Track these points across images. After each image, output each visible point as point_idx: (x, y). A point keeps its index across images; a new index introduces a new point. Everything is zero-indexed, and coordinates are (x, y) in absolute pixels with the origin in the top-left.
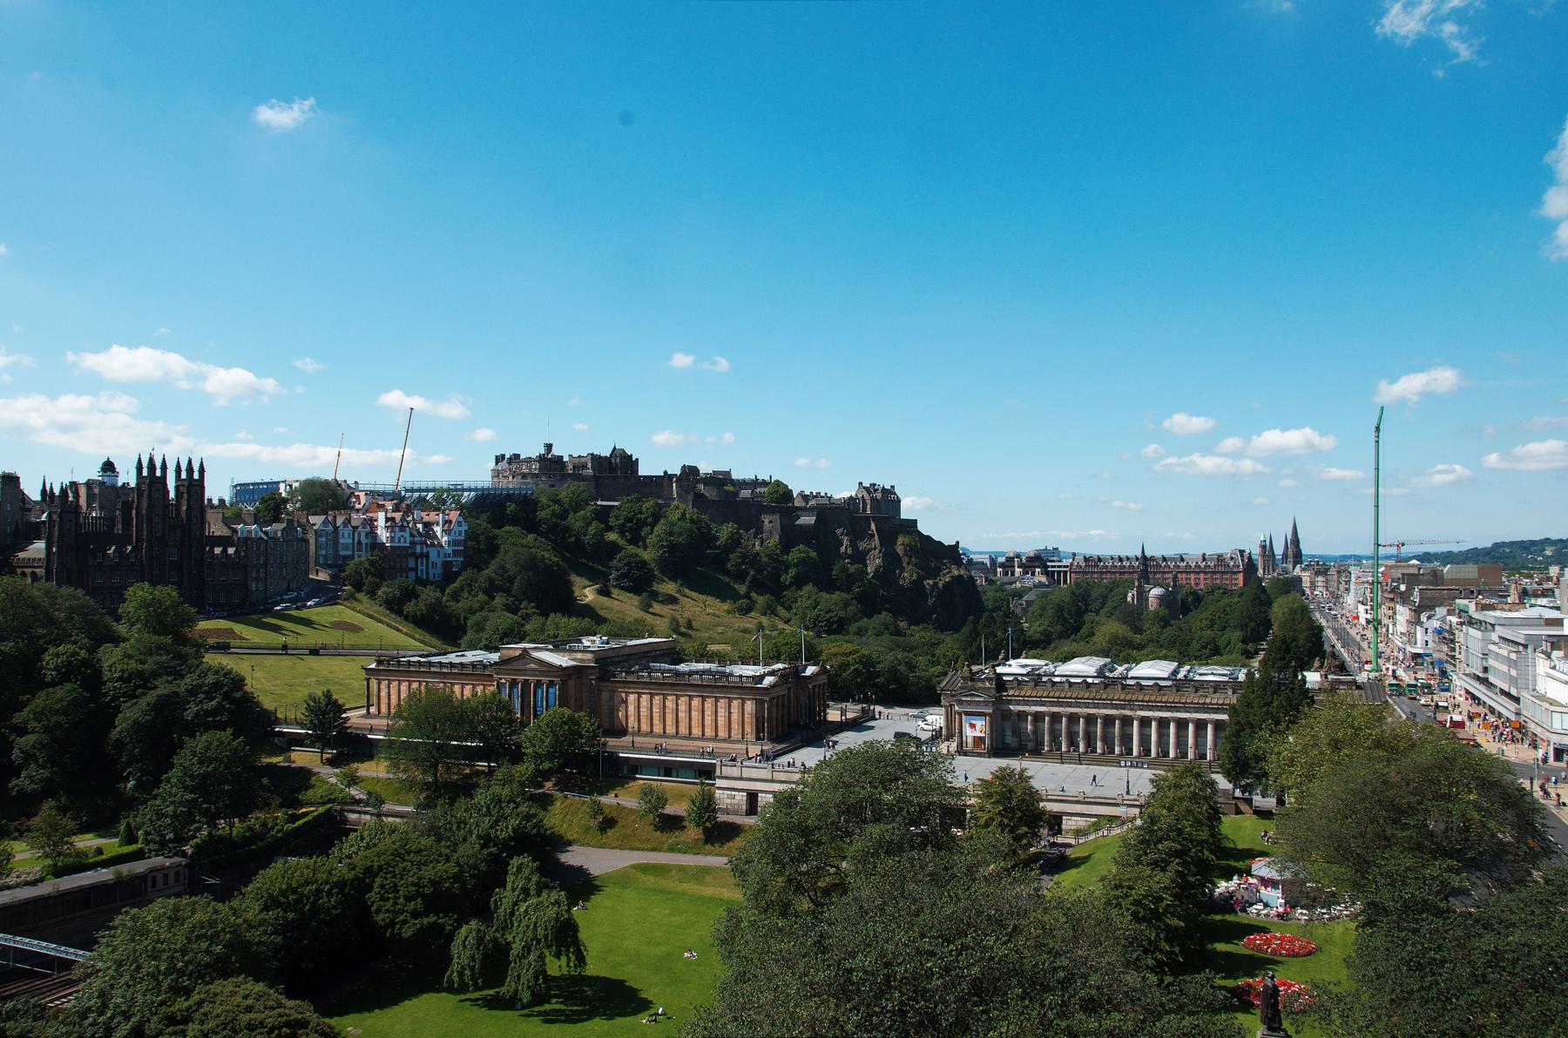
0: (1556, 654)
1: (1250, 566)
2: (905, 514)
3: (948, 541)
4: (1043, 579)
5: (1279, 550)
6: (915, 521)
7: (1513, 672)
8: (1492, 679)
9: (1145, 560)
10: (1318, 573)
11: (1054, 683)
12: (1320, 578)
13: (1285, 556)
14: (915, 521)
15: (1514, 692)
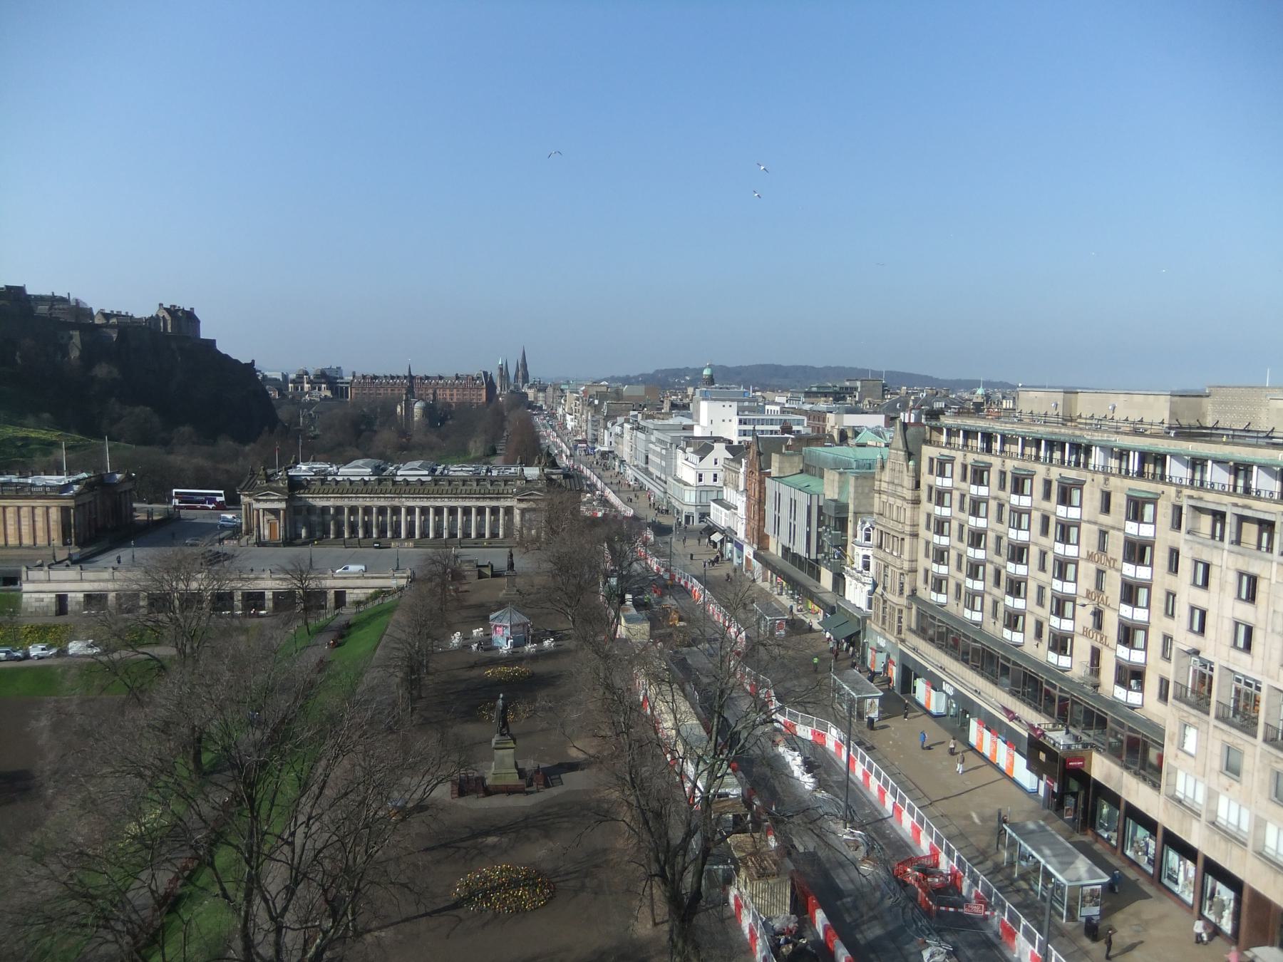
0: (689, 450)
1: (491, 386)
2: (205, 334)
3: (245, 360)
4: (329, 394)
5: (512, 373)
6: (214, 341)
7: (664, 463)
8: (651, 469)
9: (411, 378)
10: (539, 390)
11: (337, 482)
12: (541, 395)
13: (516, 376)
14: (214, 341)
15: (663, 477)
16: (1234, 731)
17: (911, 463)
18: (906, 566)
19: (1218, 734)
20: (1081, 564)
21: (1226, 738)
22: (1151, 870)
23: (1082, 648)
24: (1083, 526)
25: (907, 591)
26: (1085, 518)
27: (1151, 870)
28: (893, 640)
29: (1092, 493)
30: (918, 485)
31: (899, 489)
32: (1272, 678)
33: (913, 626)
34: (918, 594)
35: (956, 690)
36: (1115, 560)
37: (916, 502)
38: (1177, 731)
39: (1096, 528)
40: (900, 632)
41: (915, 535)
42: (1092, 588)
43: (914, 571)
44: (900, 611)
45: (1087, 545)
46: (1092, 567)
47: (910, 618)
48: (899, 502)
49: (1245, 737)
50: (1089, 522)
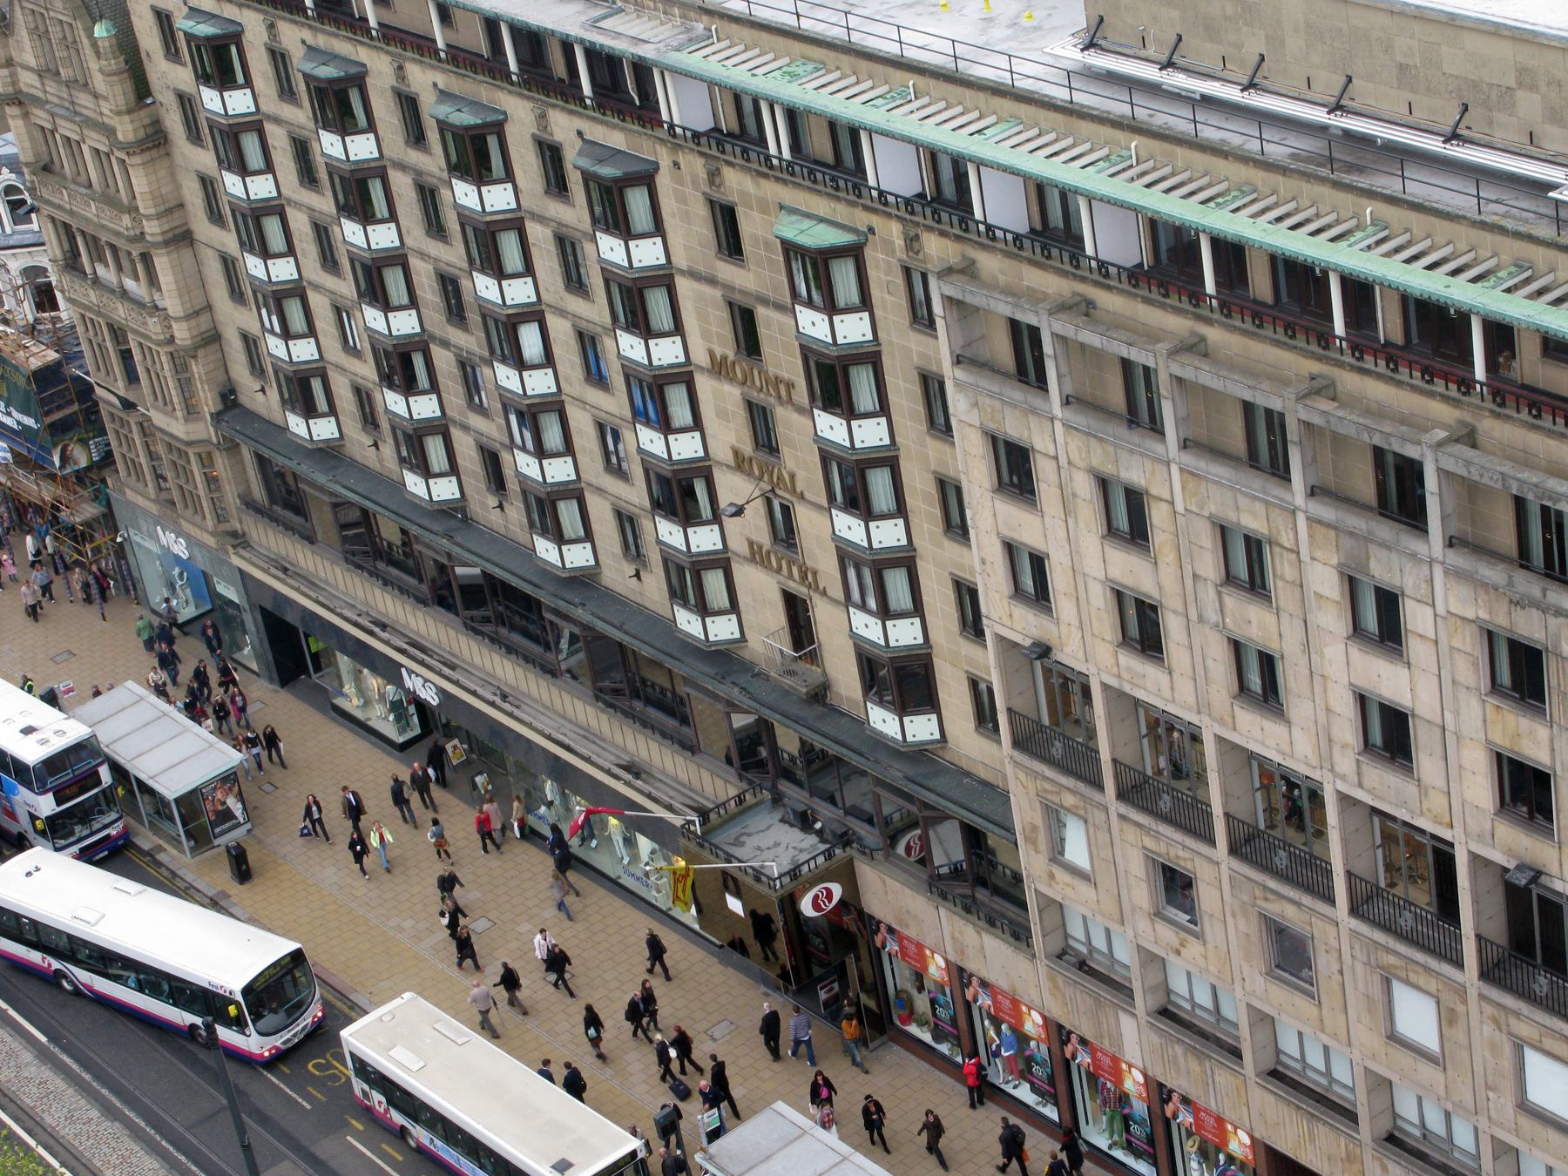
16: (1164, 829)
17: (100, 30)
18: (182, 333)
19: (1131, 834)
20: (703, 384)
21: (1149, 842)
22: (1051, 1112)
23: (761, 589)
24: (683, 285)
25: (208, 401)
26: (680, 261)
27: (1051, 1112)
28: (211, 541)
29: (682, 200)
30: (142, 90)
31: (84, 99)
32: (1221, 722)
33: (258, 492)
34: (244, 400)
35: (442, 692)
36: (790, 386)
37: (155, 140)
38: (1038, 820)
39: (717, 293)
40: (220, 518)
41: (183, 238)
42: (748, 448)
43: (213, 338)
44: (206, 461)
45: (705, 335)
46: (732, 394)
47: (238, 477)
48: (95, 140)
49: (1190, 842)
50: (693, 274)
